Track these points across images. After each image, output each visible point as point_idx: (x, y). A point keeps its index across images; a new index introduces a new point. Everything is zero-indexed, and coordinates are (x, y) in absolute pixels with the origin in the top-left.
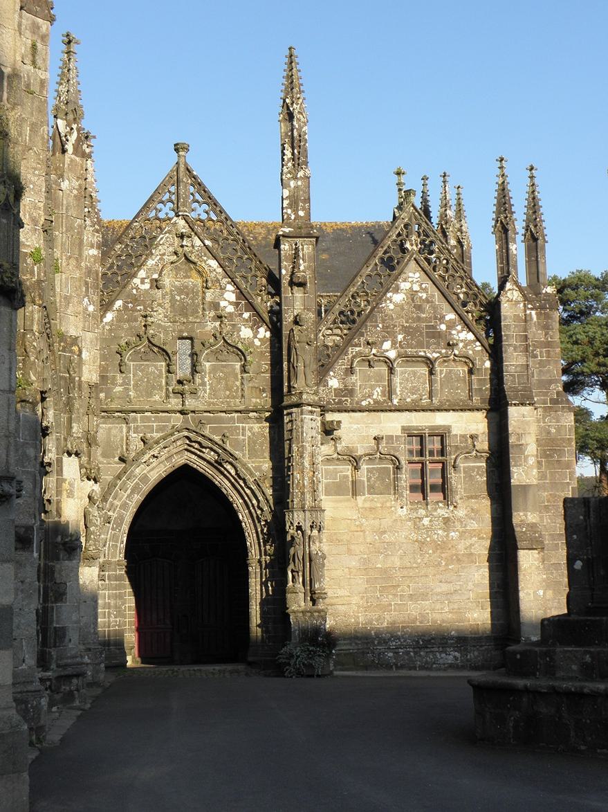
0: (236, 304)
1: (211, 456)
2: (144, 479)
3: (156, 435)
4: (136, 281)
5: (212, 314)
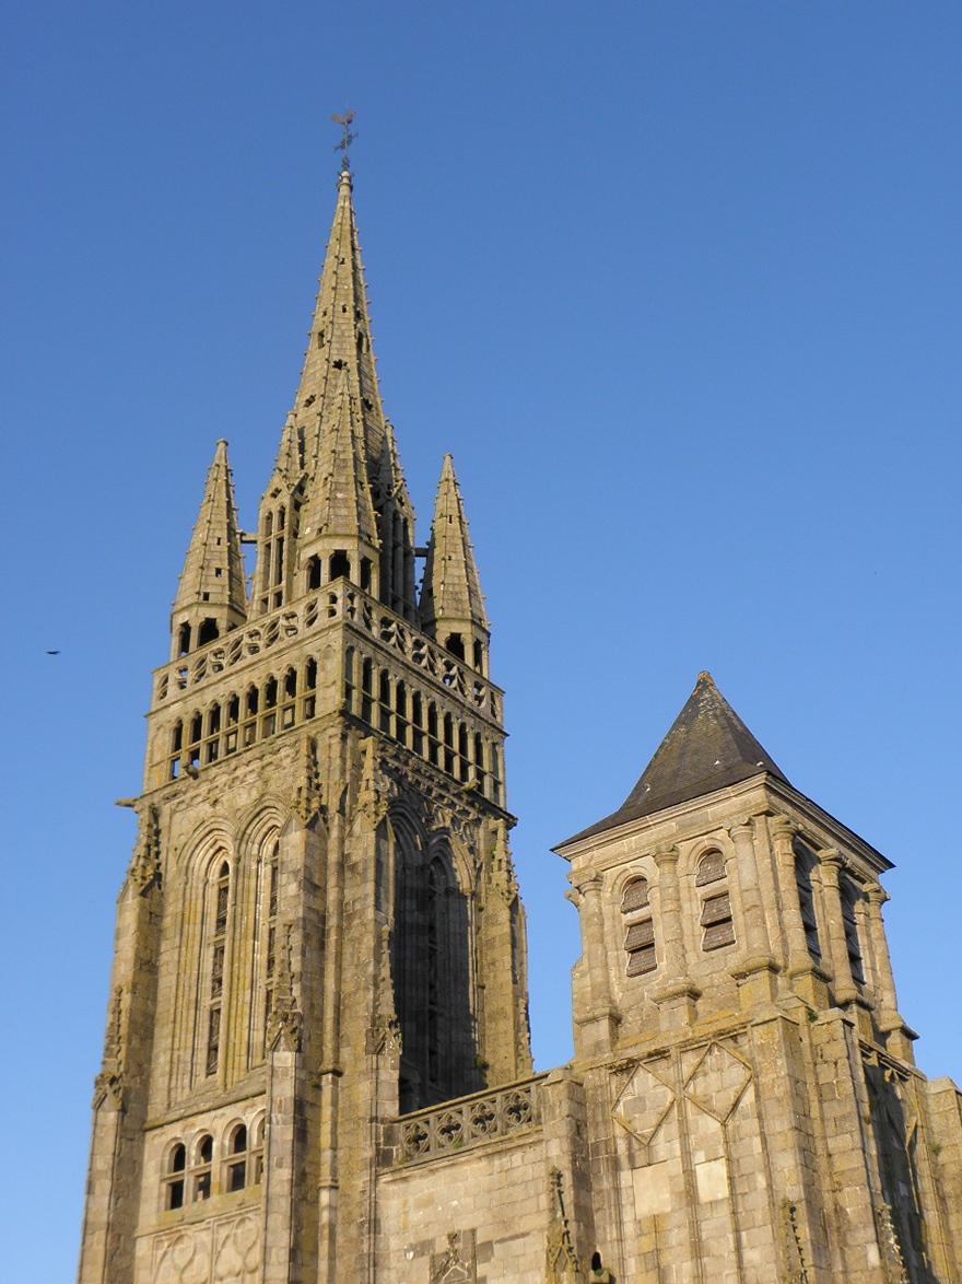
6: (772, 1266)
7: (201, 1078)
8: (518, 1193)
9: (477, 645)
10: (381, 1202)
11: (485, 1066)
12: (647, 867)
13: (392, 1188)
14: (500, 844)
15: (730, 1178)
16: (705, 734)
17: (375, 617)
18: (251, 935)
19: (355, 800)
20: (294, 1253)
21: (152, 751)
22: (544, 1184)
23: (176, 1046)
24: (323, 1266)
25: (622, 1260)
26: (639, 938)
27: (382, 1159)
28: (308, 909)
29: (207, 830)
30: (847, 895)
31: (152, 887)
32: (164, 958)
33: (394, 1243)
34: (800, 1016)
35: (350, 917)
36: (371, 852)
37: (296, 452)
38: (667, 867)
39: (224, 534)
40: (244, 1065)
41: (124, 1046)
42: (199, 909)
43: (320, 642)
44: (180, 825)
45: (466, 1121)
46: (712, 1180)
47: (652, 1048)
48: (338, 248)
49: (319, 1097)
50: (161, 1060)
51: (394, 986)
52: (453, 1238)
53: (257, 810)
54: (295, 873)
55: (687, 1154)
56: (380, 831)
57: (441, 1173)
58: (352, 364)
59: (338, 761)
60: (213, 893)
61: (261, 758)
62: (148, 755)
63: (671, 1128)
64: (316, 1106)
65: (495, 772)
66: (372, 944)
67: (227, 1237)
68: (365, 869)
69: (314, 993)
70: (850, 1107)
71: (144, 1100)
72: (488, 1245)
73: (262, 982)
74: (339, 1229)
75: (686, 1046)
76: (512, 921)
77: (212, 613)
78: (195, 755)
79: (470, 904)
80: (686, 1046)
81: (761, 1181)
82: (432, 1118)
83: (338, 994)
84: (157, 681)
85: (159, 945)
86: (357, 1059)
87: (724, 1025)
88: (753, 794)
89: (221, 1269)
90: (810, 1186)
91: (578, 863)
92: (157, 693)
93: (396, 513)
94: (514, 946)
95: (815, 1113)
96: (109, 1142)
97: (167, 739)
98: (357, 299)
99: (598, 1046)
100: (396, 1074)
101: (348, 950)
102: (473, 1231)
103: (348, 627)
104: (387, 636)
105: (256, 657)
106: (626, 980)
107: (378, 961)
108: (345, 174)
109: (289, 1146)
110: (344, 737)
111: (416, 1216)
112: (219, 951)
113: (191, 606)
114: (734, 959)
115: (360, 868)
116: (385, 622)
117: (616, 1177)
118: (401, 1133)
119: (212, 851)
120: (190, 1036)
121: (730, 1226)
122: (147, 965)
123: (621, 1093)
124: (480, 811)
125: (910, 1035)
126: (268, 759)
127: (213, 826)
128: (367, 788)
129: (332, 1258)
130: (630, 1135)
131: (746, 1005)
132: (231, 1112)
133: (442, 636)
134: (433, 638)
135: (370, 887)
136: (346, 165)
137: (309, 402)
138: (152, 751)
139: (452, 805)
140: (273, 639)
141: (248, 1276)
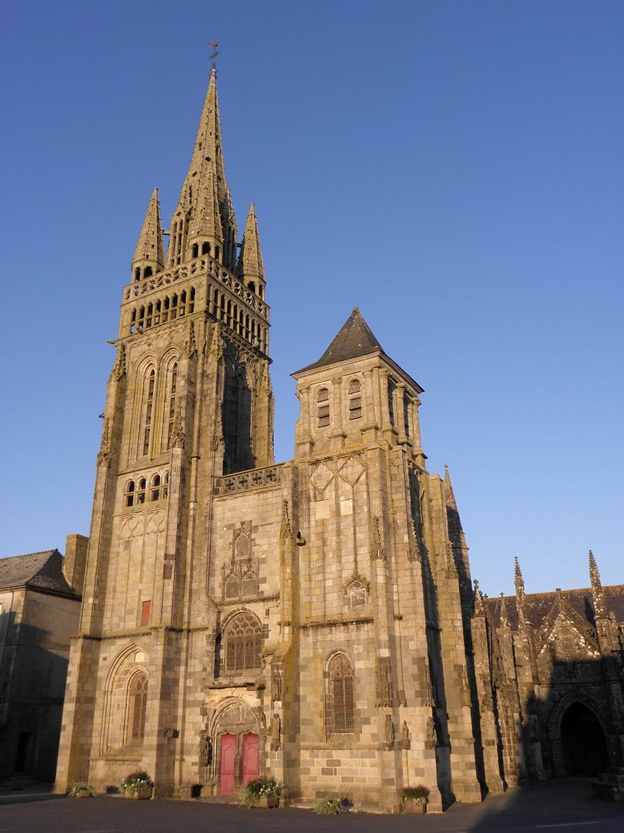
0: (585, 643)
1: (585, 699)
2: (563, 708)
3: (564, 692)
4: (550, 638)
5: (577, 647)
6: (367, 540)
7: (141, 456)
8: (269, 508)
9: (261, 287)
10: (214, 508)
11: (255, 458)
12: (329, 385)
13: (219, 503)
14: (266, 370)
15: (354, 507)
16: (355, 332)
17: (220, 272)
18: (163, 400)
19: (209, 348)
20: (179, 526)
21: (123, 321)
22: (281, 505)
23: (131, 443)
24: (190, 531)
25: (309, 537)
26: (324, 412)
27: (215, 492)
28: (189, 392)
30: (406, 401)
31: (122, 378)
32: (127, 407)
33: (219, 524)
34: (386, 448)
35: (206, 396)
36: (215, 370)
37: (188, 196)
38: (337, 385)
39: (156, 230)
40: (159, 452)
41: (110, 442)
42: (142, 387)
43: (197, 281)
44: (134, 353)
45: (250, 479)
46: (346, 507)
47: (326, 456)
48: (208, 105)
49: (190, 466)
50: (125, 448)
51: (222, 425)
52: (243, 523)
54: (184, 376)
55: (337, 497)
56: (219, 362)
57: (238, 499)
58: (213, 159)
59: (203, 332)
60: (147, 382)
61: (170, 328)
62: (121, 323)
63: (332, 487)
64: (189, 470)
65: (265, 341)
66: (214, 407)
67: (151, 518)
68: (212, 377)
69: (190, 425)
70: (402, 483)
71: (118, 463)
72: (257, 527)
73: (168, 419)
74: (197, 518)
75: (340, 456)
76: (269, 402)
77: (150, 264)
78: (141, 324)
79: (252, 394)
80: (340, 456)
81: (366, 509)
82: (236, 477)
83: (200, 426)
84: (125, 291)
85: (124, 402)
86: (206, 453)
87: (356, 449)
88: (374, 359)
89: (149, 530)
90: (385, 512)
91: (301, 381)
92: (125, 296)
93: (230, 227)
94: (269, 412)
95: (388, 484)
96: (103, 479)
97: (130, 316)
98: (216, 129)
99: (304, 454)
100: (222, 459)
101: (204, 409)
102: (251, 521)
103: (209, 275)
104: (224, 280)
105: (169, 285)
107: (216, 414)
108: (213, 70)
109: (178, 485)
110: (206, 322)
111: (228, 514)
112: (150, 406)
113: (141, 260)
114: (361, 424)
116: (224, 275)
117: (309, 504)
118: (223, 482)
119: (148, 365)
120: (137, 439)
121: (352, 524)
122: (120, 410)
123: (313, 471)
124: (258, 356)
125: (425, 457)
126: (172, 329)
128: (214, 344)
129: (194, 528)
130: (315, 489)
131: (365, 441)
132: (154, 470)
133: (246, 282)
134: (242, 283)
135: (214, 384)
136: (214, 66)
137: (194, 175)
138: (123, 321)
139: (247, 353)
140: (177, 278)
141: (159, 534)
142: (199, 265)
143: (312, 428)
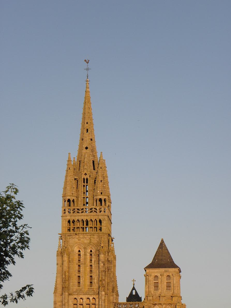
12: (159, 275)
29: (78, 244)
53: (89, 244)
54: (103, 262)
80: (164, 304)
86: (110, 293)
106: (154, 291)
115: (110, 261)
127: (79, 244)
142: (102, 210)
143: (152, 290)
